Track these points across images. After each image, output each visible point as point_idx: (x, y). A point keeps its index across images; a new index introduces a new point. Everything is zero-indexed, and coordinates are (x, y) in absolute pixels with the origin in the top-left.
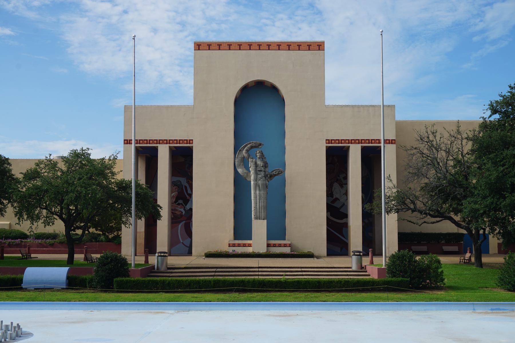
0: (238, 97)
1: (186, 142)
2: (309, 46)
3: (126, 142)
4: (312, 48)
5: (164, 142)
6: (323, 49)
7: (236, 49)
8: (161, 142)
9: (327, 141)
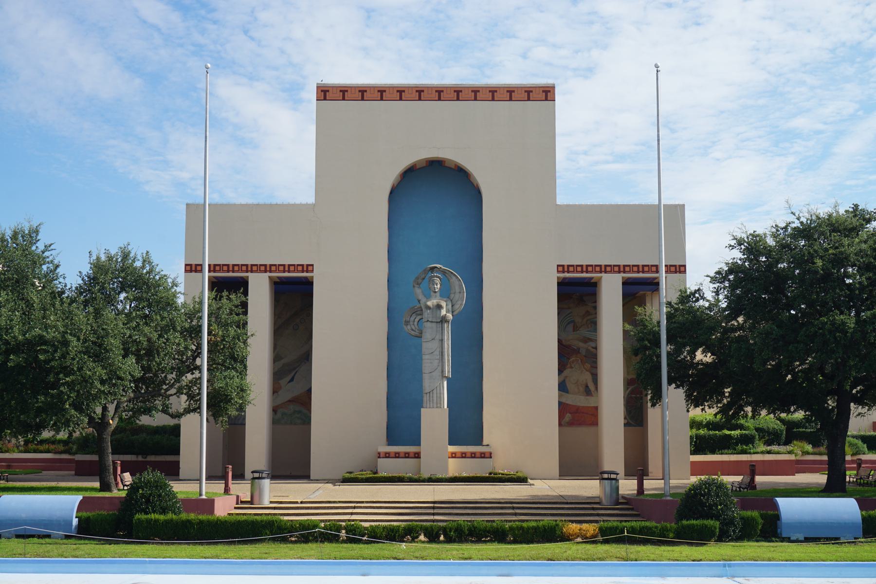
0: (395, 186)
3: (188, 268)
5: (243, 270)
8: (255, 268)
9: (559, 267)
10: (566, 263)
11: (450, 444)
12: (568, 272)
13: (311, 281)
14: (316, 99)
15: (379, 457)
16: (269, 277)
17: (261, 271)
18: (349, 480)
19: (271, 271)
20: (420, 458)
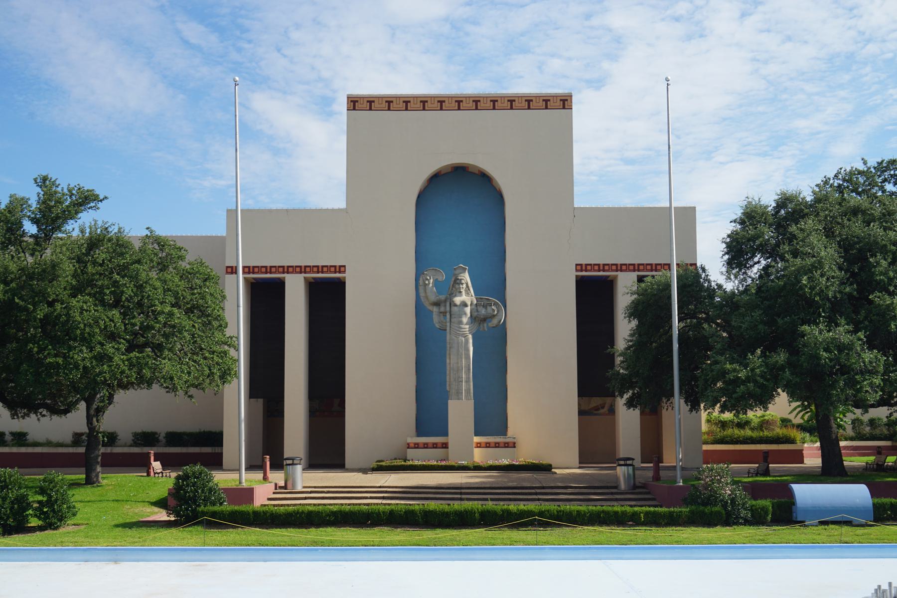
1: (316, 271)
2: (546, 102)
4: (482, 105)
6: (569, 107)
7: (418, 109)
9: (577, 266)
10: (584, 262)
11: (477, 434)
12: (586, 271)
13: (343, 281)
14: (346, 109)
15: (408, 448)
16: (304, 278)
17: (297, 273)
18: (380, 469)
19: (305, 272)
20: (448, 448)
